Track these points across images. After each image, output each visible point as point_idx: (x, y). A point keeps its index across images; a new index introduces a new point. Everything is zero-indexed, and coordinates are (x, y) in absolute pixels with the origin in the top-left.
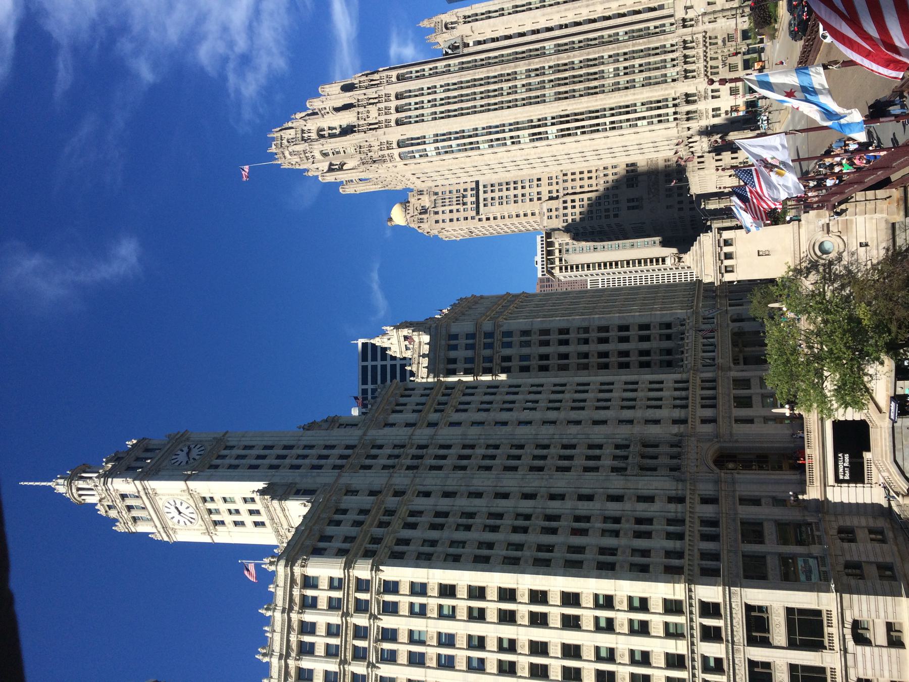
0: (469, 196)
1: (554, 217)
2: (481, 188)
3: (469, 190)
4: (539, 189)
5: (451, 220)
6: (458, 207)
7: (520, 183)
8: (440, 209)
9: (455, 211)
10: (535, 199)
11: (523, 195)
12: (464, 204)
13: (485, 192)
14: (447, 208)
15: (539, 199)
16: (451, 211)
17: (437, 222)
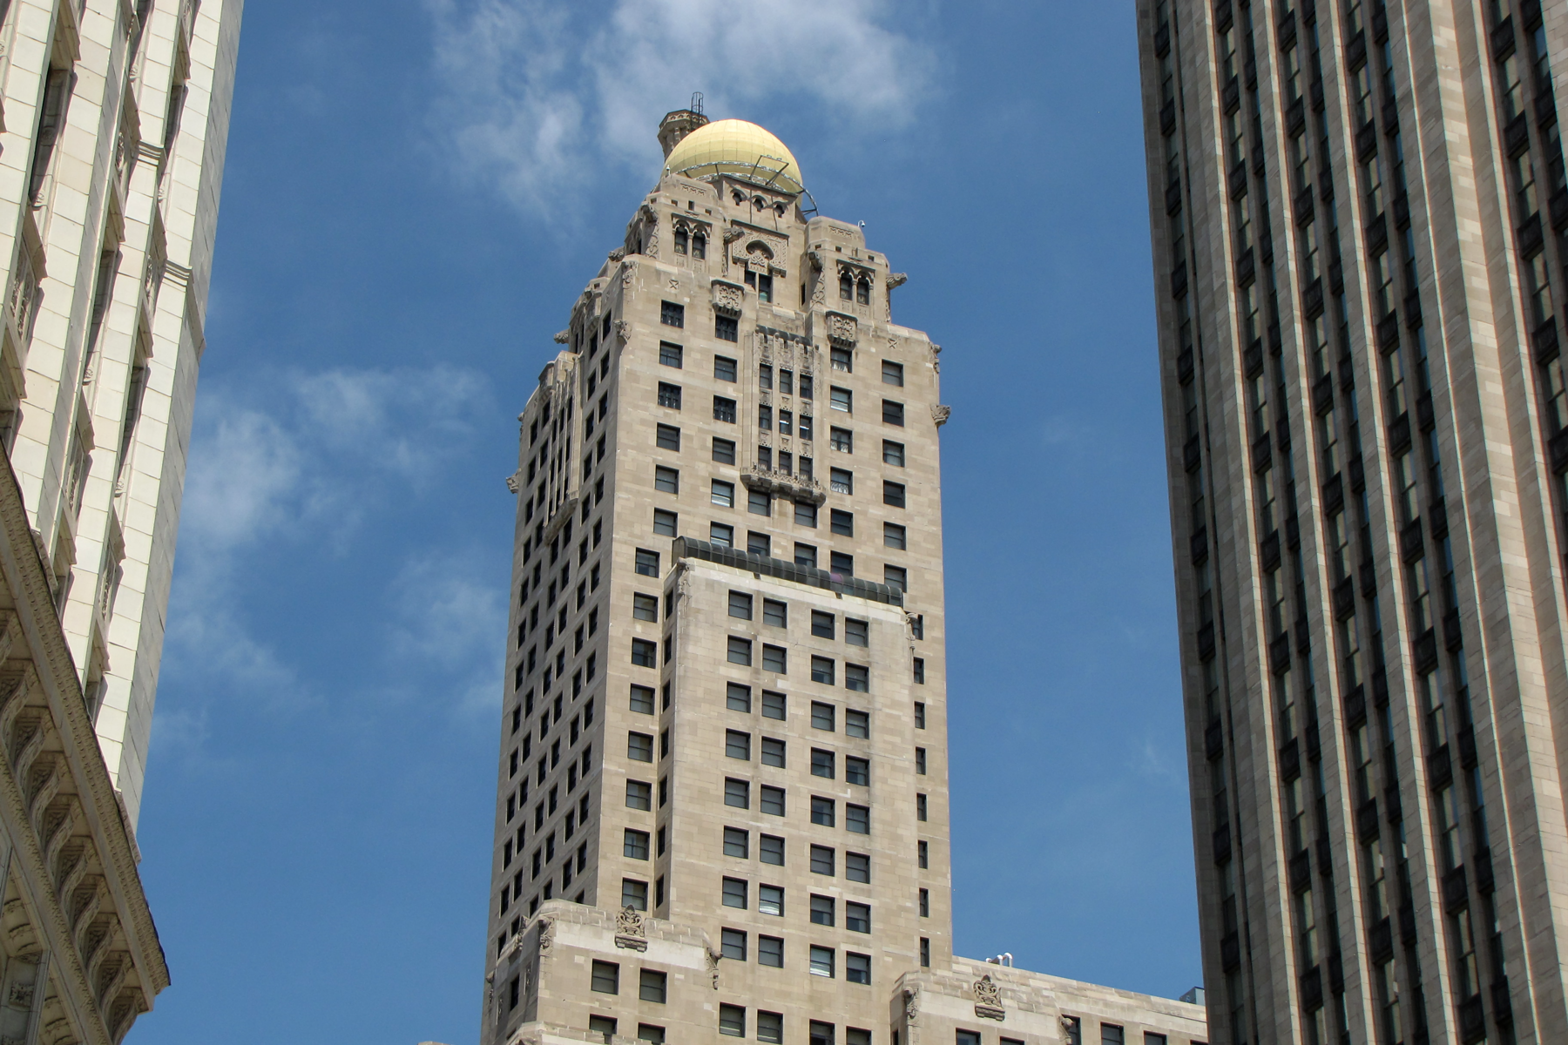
0: (807, 535)
1: (605, 1004)
2: (853, 606)
3: (843, 545)
4: (796, 954)
5: (670, 394)
6: (747, 456)
7: (857, 843)
8: (745, 352)
9: (725, 430)
10: (736, 918)
11: (774, 847)
12: (762, 494)
13: (823, 624)
14: (745, 392)
15: (734, 938)
16: (724, 408)
17: (672, 312)
